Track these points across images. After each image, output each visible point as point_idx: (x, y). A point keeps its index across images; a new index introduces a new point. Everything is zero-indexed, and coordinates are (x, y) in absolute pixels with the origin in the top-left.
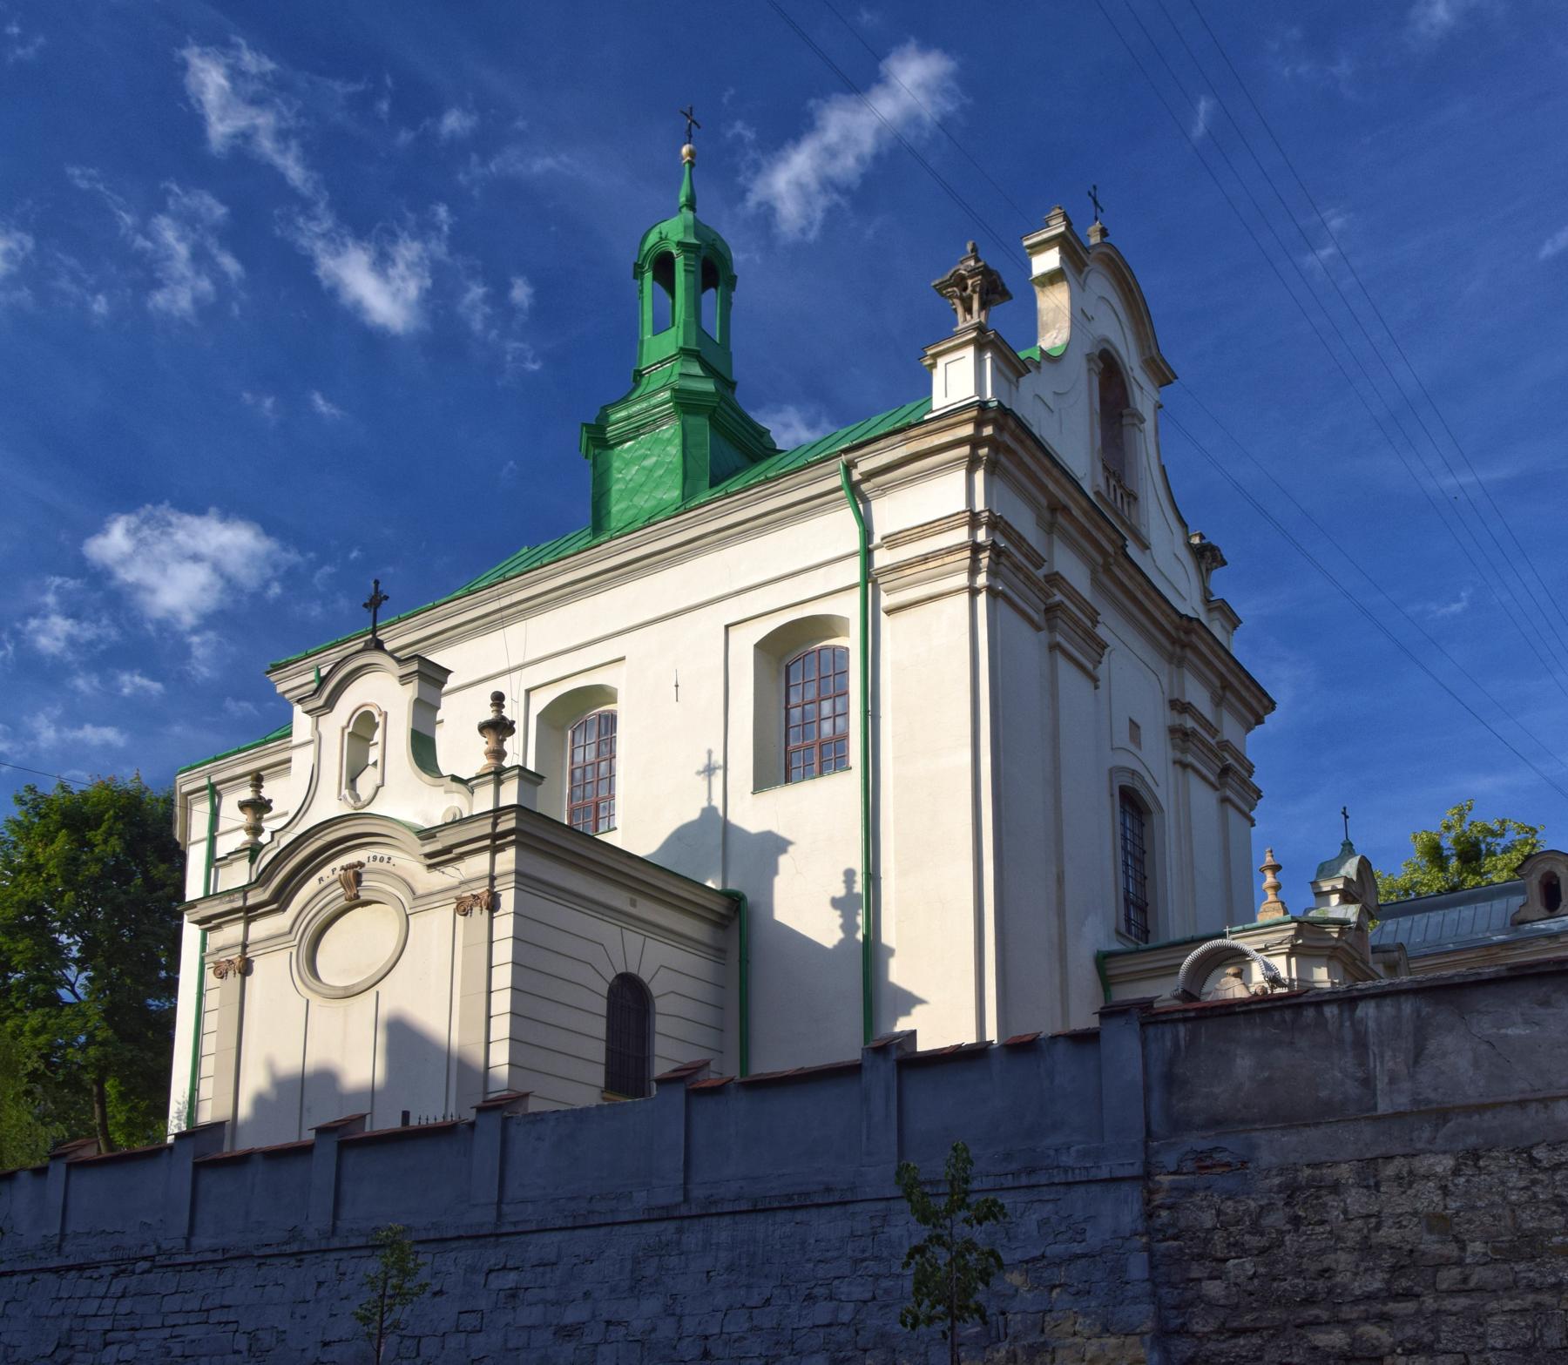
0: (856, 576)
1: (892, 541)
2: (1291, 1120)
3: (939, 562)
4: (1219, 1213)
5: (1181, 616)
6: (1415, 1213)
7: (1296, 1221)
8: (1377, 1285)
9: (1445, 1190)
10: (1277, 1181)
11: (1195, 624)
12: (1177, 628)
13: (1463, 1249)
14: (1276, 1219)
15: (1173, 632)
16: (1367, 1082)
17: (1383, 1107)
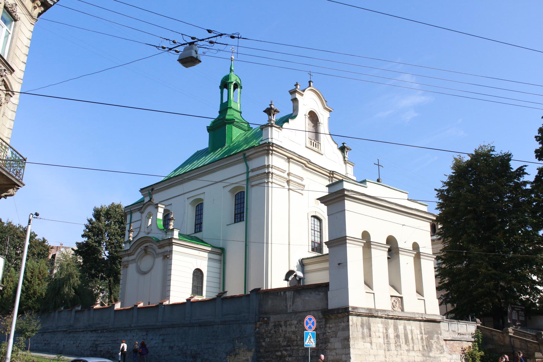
0: (246, 178)
1: (253, 170)
2: (276, 313)
3: (260, 176)
4: (265, 330)
5: (331, 171)
6: (291, 331)
7: (275, 332)
8: (285, 344)
9: (296, 327)
10: (273, 324)
12: (330, 174)
13: (297, 338)
14: (272, 332)
15: (329, 175)
16: (286, 307)
17: (289, 311)
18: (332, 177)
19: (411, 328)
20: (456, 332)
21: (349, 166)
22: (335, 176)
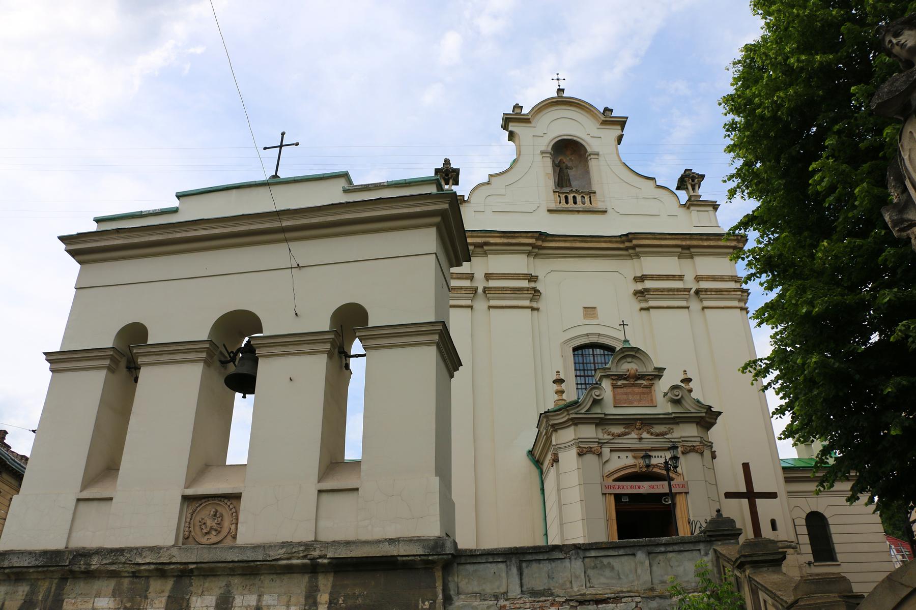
5: (620, 236)
11: (630, 236)
15: (621, 246)
18: (634, 248)
19: (259, 600)
20: (552, 595)
21: (698, 211)
22: (635, 242)
